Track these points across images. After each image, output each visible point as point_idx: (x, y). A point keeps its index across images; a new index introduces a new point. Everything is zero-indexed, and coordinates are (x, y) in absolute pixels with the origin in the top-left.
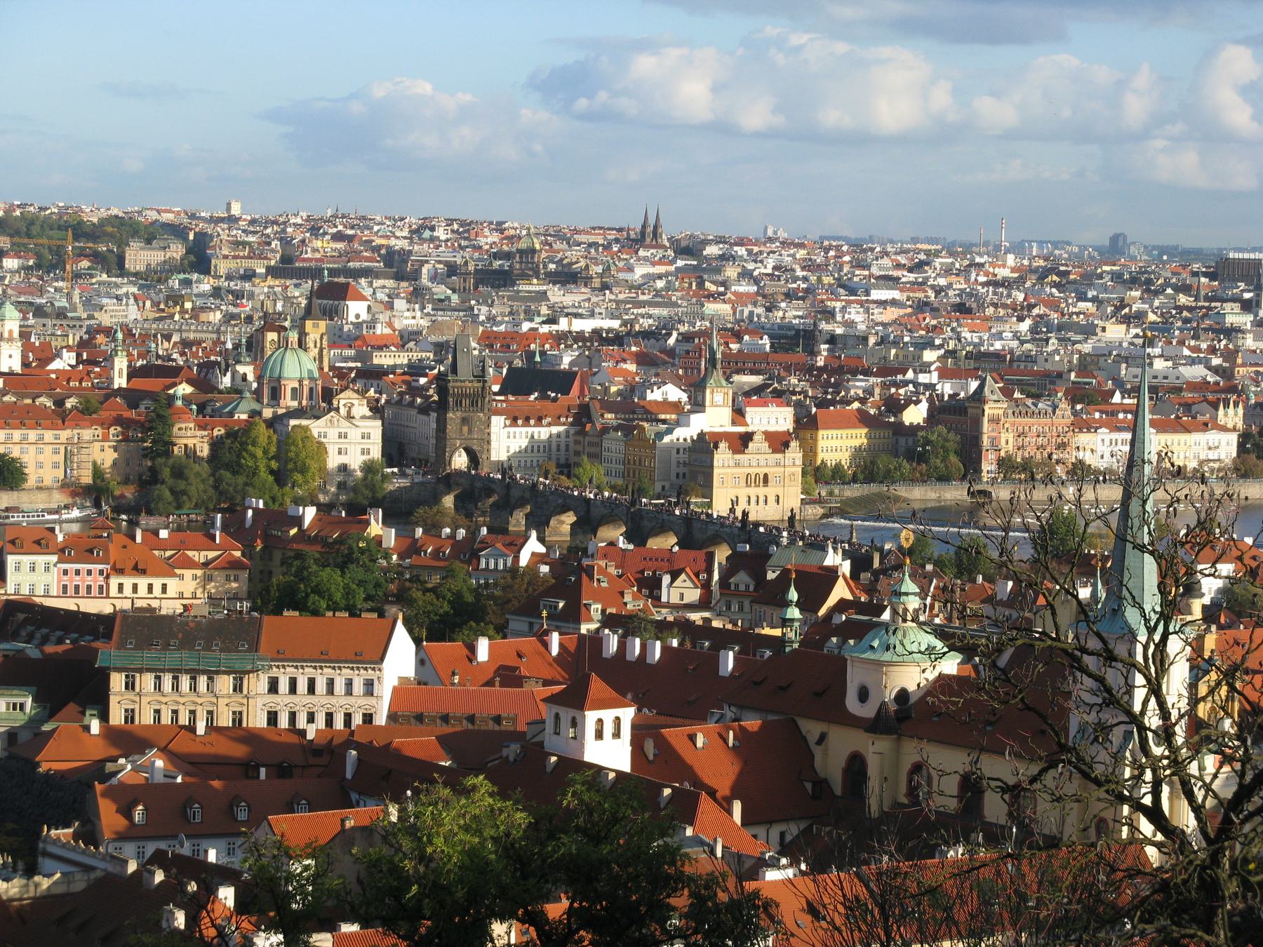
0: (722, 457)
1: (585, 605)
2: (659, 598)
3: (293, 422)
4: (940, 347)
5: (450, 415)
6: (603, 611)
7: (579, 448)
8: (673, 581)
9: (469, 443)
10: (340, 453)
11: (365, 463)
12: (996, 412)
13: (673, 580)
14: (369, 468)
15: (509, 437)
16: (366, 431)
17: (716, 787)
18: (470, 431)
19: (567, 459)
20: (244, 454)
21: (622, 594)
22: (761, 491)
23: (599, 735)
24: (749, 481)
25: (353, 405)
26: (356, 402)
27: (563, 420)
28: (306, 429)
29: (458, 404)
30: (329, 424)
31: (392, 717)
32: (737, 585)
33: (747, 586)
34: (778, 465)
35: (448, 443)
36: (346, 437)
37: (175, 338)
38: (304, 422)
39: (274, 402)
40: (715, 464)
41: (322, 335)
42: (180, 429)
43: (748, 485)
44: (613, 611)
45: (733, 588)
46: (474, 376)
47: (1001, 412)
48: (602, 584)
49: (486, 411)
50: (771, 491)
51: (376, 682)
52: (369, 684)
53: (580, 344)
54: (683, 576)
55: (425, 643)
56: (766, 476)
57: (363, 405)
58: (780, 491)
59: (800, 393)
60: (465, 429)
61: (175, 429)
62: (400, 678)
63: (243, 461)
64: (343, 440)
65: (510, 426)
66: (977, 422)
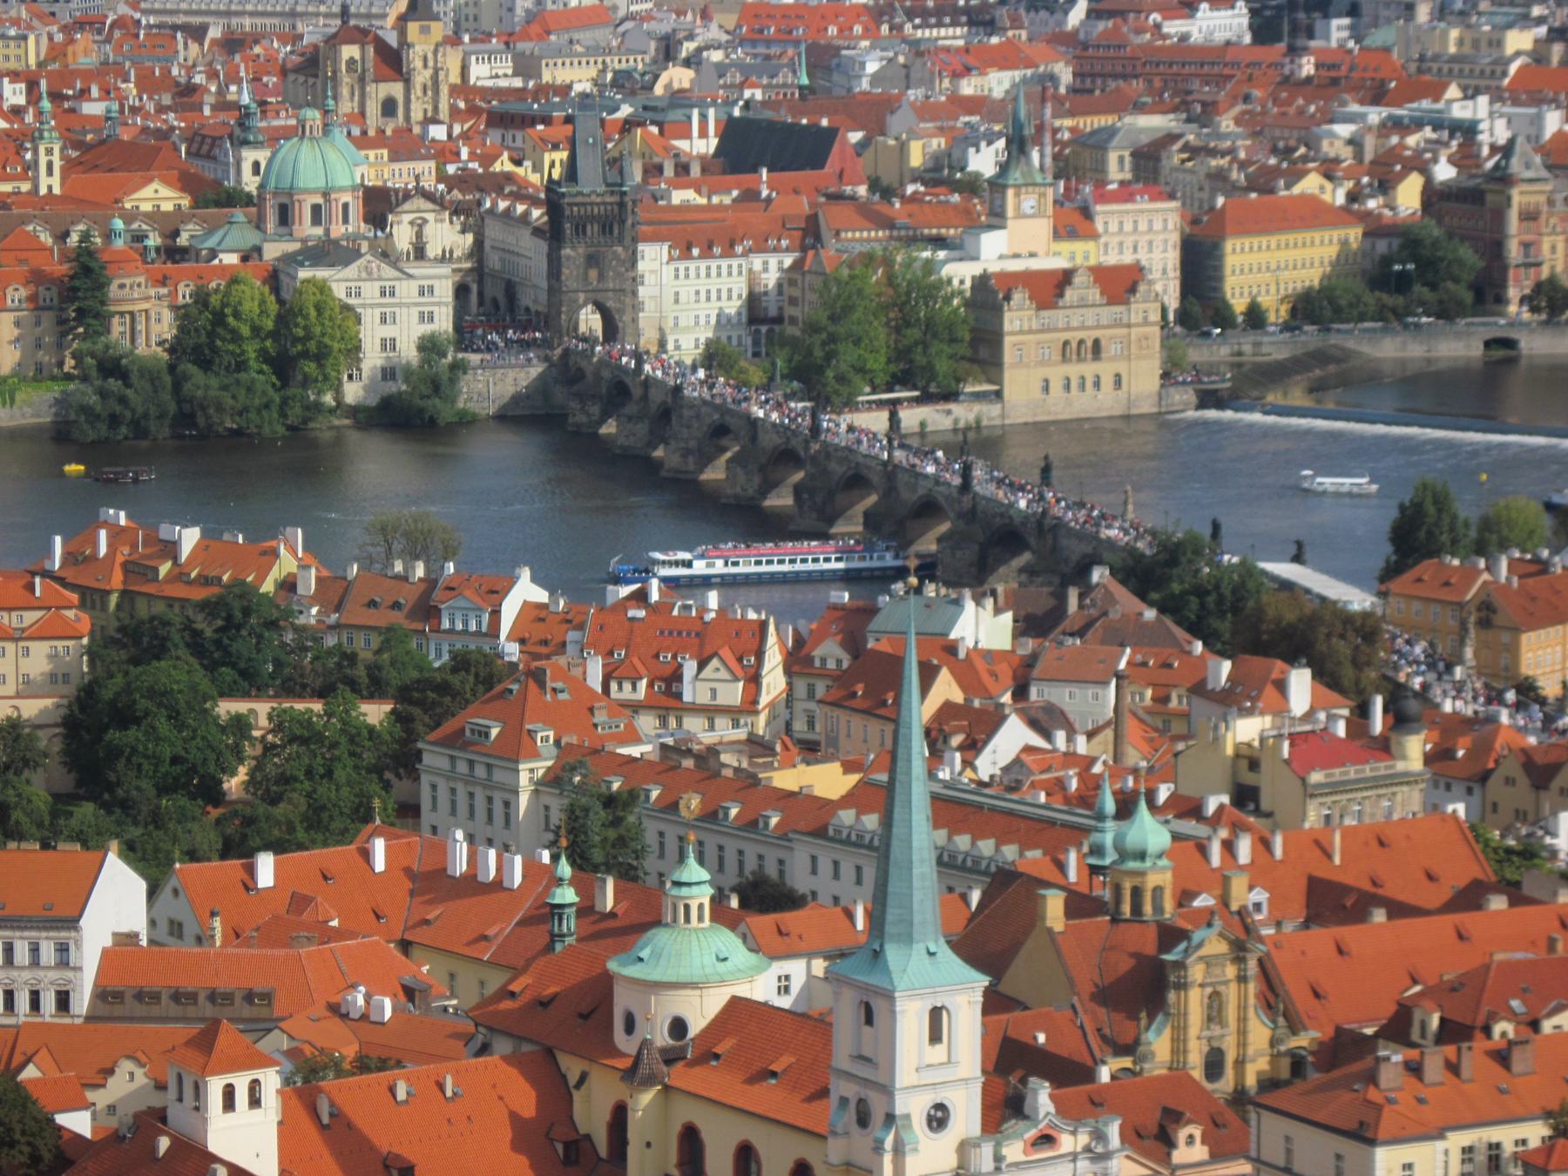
0: (1017, 318)
1: (529, 731)
2: (679, 696)
3: (303, 274)
4: (1540, 21)
5: (567, 251)
6: (557, 742)
7: (796, 293)
8: (701, 666)
9: (600, 297)
10: (383, 320)
11: (422, 338)
12: (1533, 199)
13: (701, 666)
14: (429, 346)
15: (677, 277)
16: (426, 283)
17: (413, 1159)
18: (601, 277)
19: (781, 309)
20: (220, 330)
21: (591, 710)
22: (1089, 369)
23: (229, 1103)
24: (1067, 352)
25: (425, 221)
26: (430, 217)
27: (772, 242)
28: (323, 288)
29: (580, 229)
30: (364, 275)
31: (102, 994)
32: (823, 660)
33: (839, 662)
34: (1117, 324)
35: (565, 298)
36: (392, 294)
37: (215, 33)
38: (321, 273)
39: (283, 230)
40: (1007, 327)
41: (437, 45)
42: (122, 286)
43: (1065, 358)
44: (574, 740)
45: (817, 663)
46: (608, 185)
47: (1542, 199)
48: (562, 697)
49: (628, 240)
50: (1106, 370)
51: (72, 948)
52: (63, 949)
53: (917, 21)
54: (715, 663)
55: (178, 865)
56: (1097, 343)
57: (442, 221)
58: (1122, 367)
59: (1223, 154)
60: (593, 273)
61: (114, 287)
62: (115, 935)
63: (219, 343)
64: (387, 300)
65: (679, 259)
66: (1499, 216)
